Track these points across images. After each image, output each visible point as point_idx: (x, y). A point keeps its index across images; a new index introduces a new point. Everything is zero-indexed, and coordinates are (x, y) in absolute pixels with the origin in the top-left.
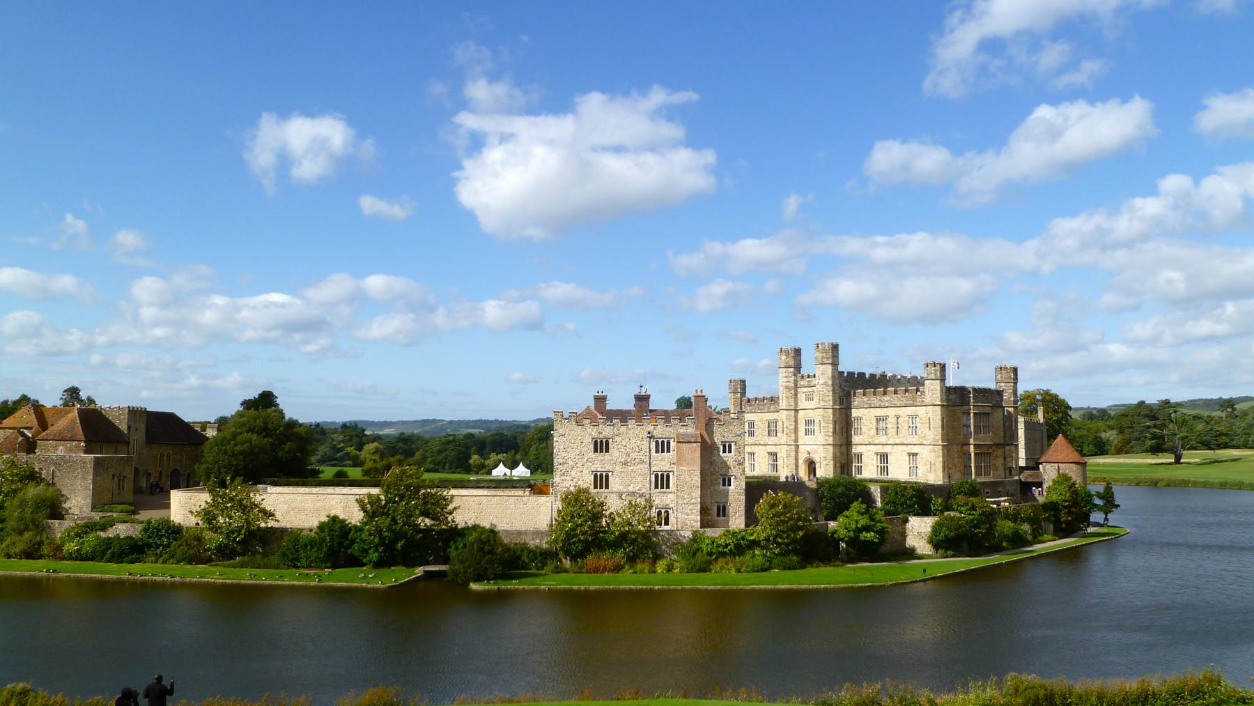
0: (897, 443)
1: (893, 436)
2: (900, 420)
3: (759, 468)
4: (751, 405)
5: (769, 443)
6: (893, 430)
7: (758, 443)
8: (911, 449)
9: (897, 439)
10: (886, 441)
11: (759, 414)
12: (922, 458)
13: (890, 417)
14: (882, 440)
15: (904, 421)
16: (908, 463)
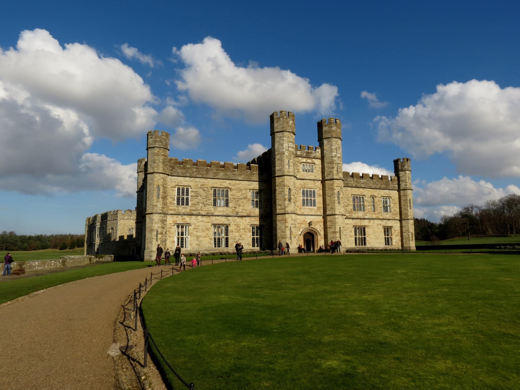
0: (373, 218)
1: (369, 212)
2: (376, 199)
3: (196, 242)
4: (184, 168)
5: (216, 214)
6: (370, 207)
7: (195, 213)
8: (386, 223)
9: (373, 215)
10: (363, 216)
11: (197, 180)
12: (395, 231)
13: (367, 197)
14: (359, 215)
15: (379, 201)
16: (383, 235)
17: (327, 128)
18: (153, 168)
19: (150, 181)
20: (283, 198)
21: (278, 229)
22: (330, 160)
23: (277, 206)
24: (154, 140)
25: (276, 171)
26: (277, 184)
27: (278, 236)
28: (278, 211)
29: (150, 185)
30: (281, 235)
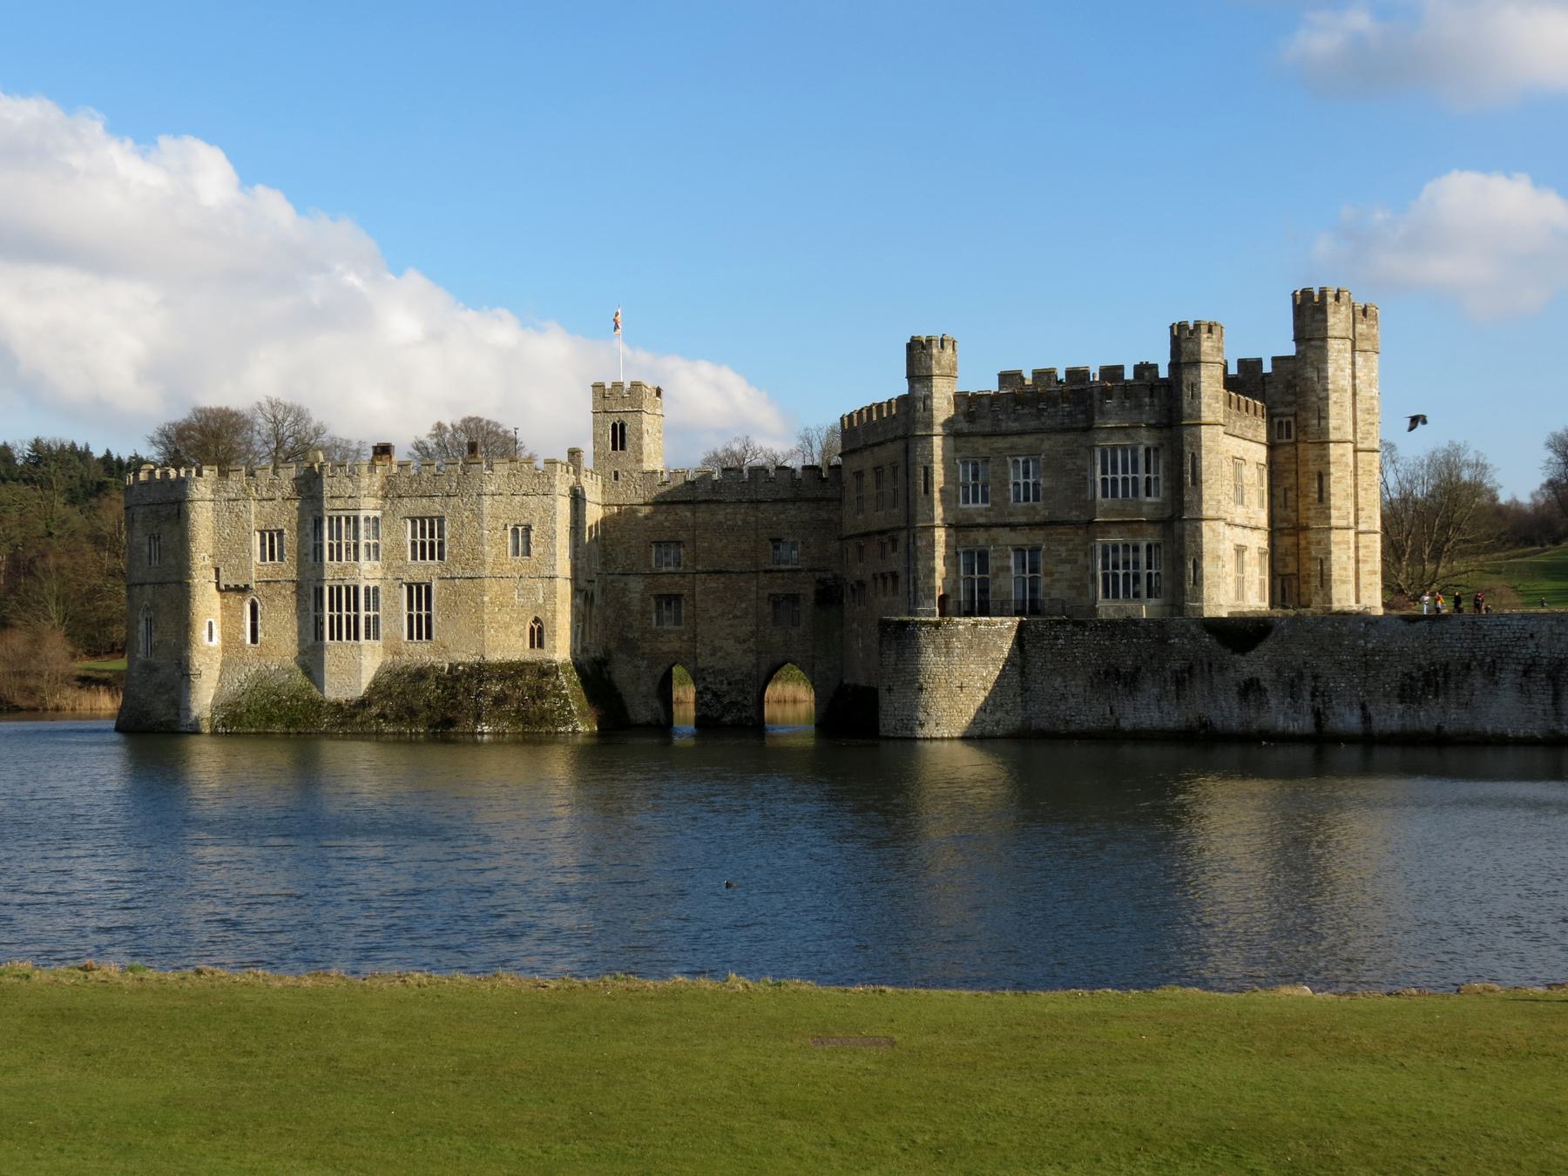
17: (1364, 326)
18: (1213, 412)
19: (1208, 443)
20: (1345, 494)
21: (1333, 562)
22: (1368, 406)
23: (1332, 511)
24: (1216, 345)
25: (1331, 430)
26: (1332, 459)
27: (1333, 578)
28: (1334, 522)
29: (1209, 452)
30: (1339, 575)
